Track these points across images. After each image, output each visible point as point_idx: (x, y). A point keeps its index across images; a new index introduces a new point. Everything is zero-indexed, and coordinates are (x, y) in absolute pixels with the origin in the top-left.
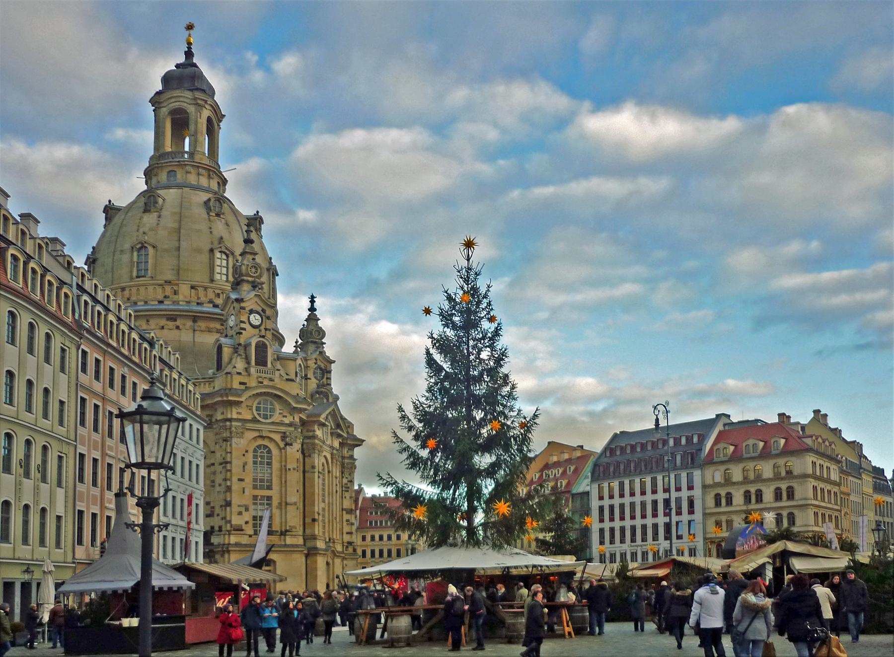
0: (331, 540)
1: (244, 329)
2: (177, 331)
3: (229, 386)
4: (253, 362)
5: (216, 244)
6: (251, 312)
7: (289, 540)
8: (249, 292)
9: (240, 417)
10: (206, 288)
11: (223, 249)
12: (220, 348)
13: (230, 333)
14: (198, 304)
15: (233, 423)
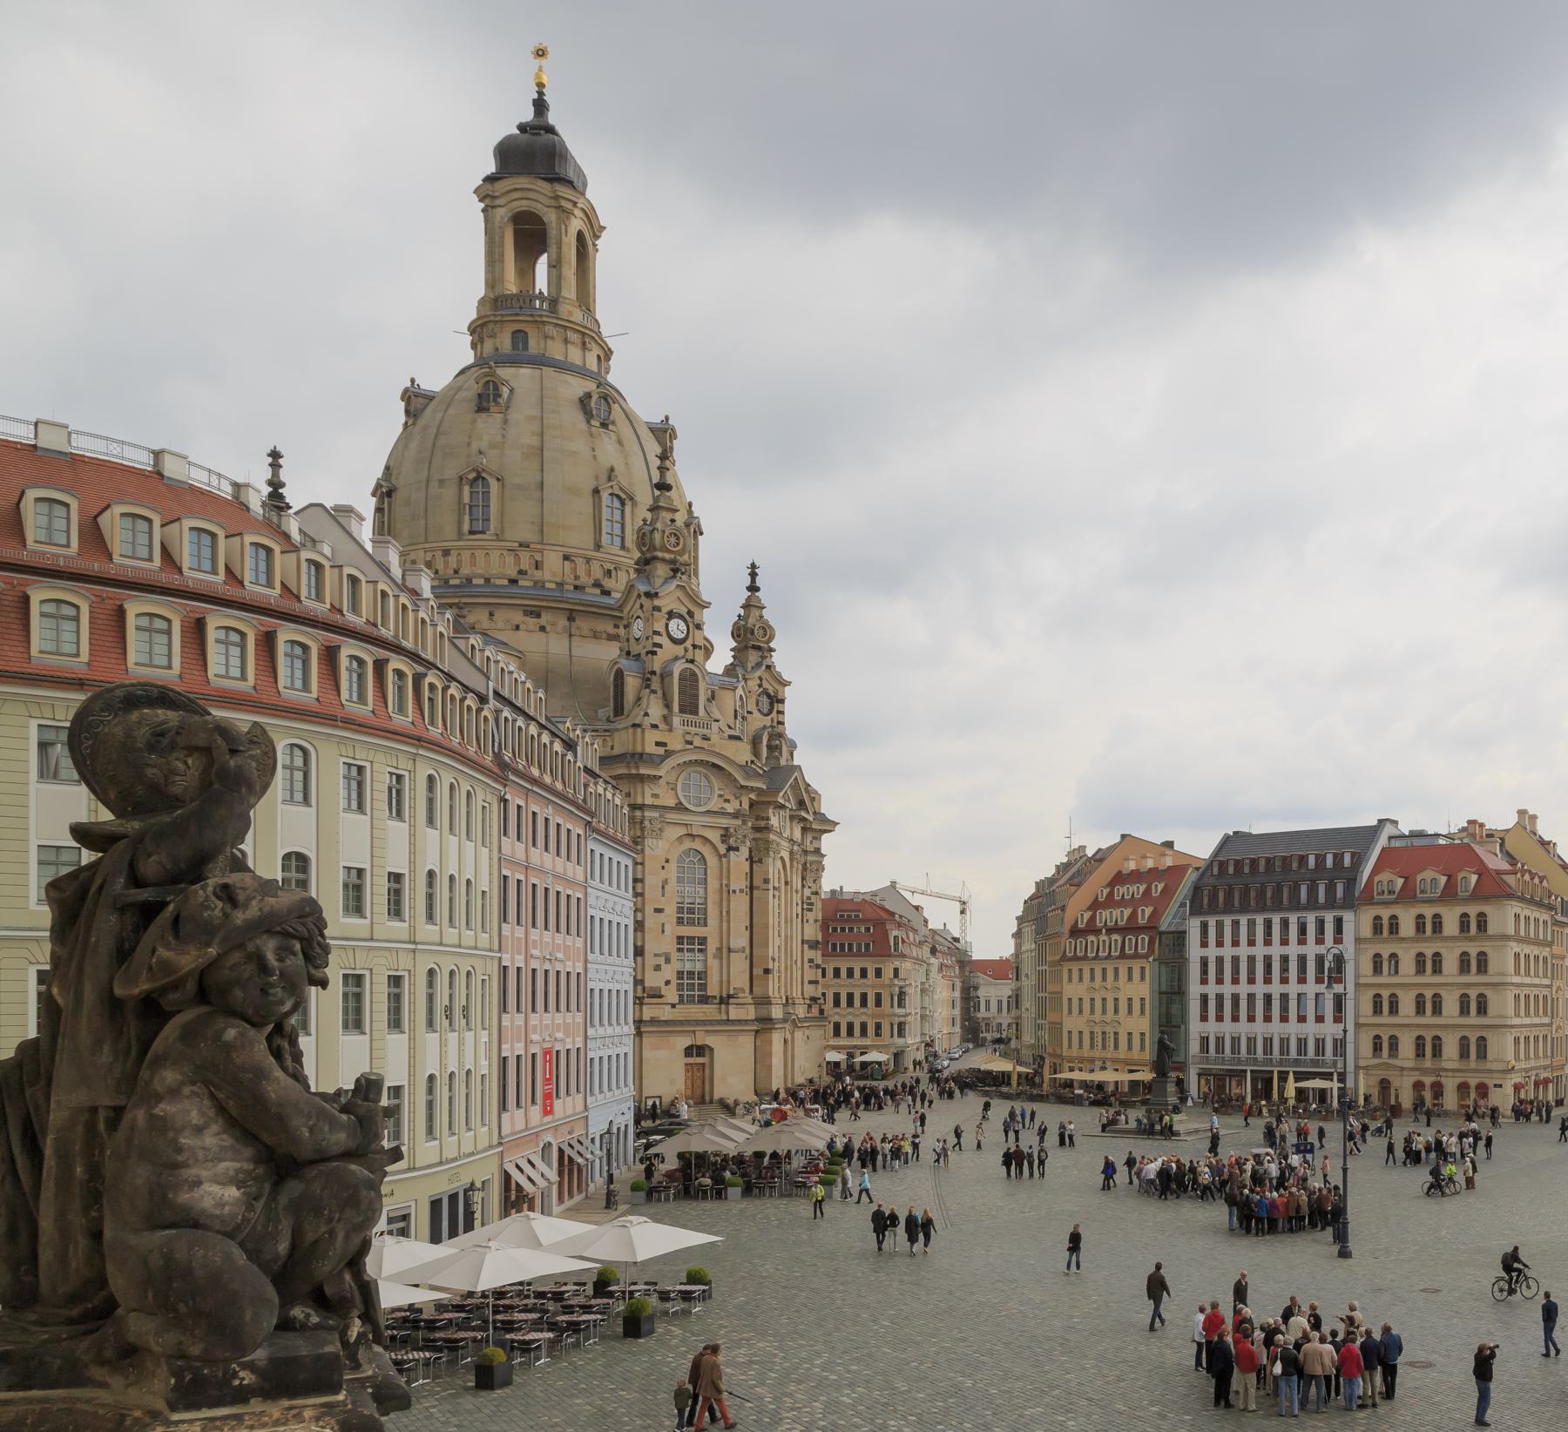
0: (788, 1002)
1: (660, 646)
2: (542, 635)
3: (639, 749)
4: (676, 708)
5: (603, 478)
6: (671, 615)
7: (735, 1013)
8: (666, 581)
9: (657, 802)
10: (588, 560)
11: (617, 492)
12: (619, 676)
13: (635, 649)
14: (576, 587)
15: (648, 814)
